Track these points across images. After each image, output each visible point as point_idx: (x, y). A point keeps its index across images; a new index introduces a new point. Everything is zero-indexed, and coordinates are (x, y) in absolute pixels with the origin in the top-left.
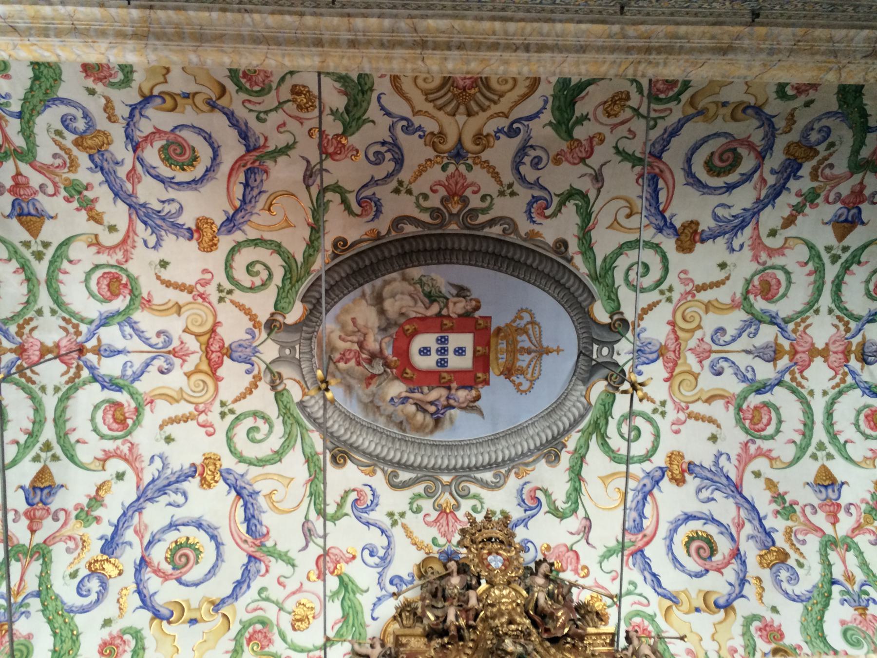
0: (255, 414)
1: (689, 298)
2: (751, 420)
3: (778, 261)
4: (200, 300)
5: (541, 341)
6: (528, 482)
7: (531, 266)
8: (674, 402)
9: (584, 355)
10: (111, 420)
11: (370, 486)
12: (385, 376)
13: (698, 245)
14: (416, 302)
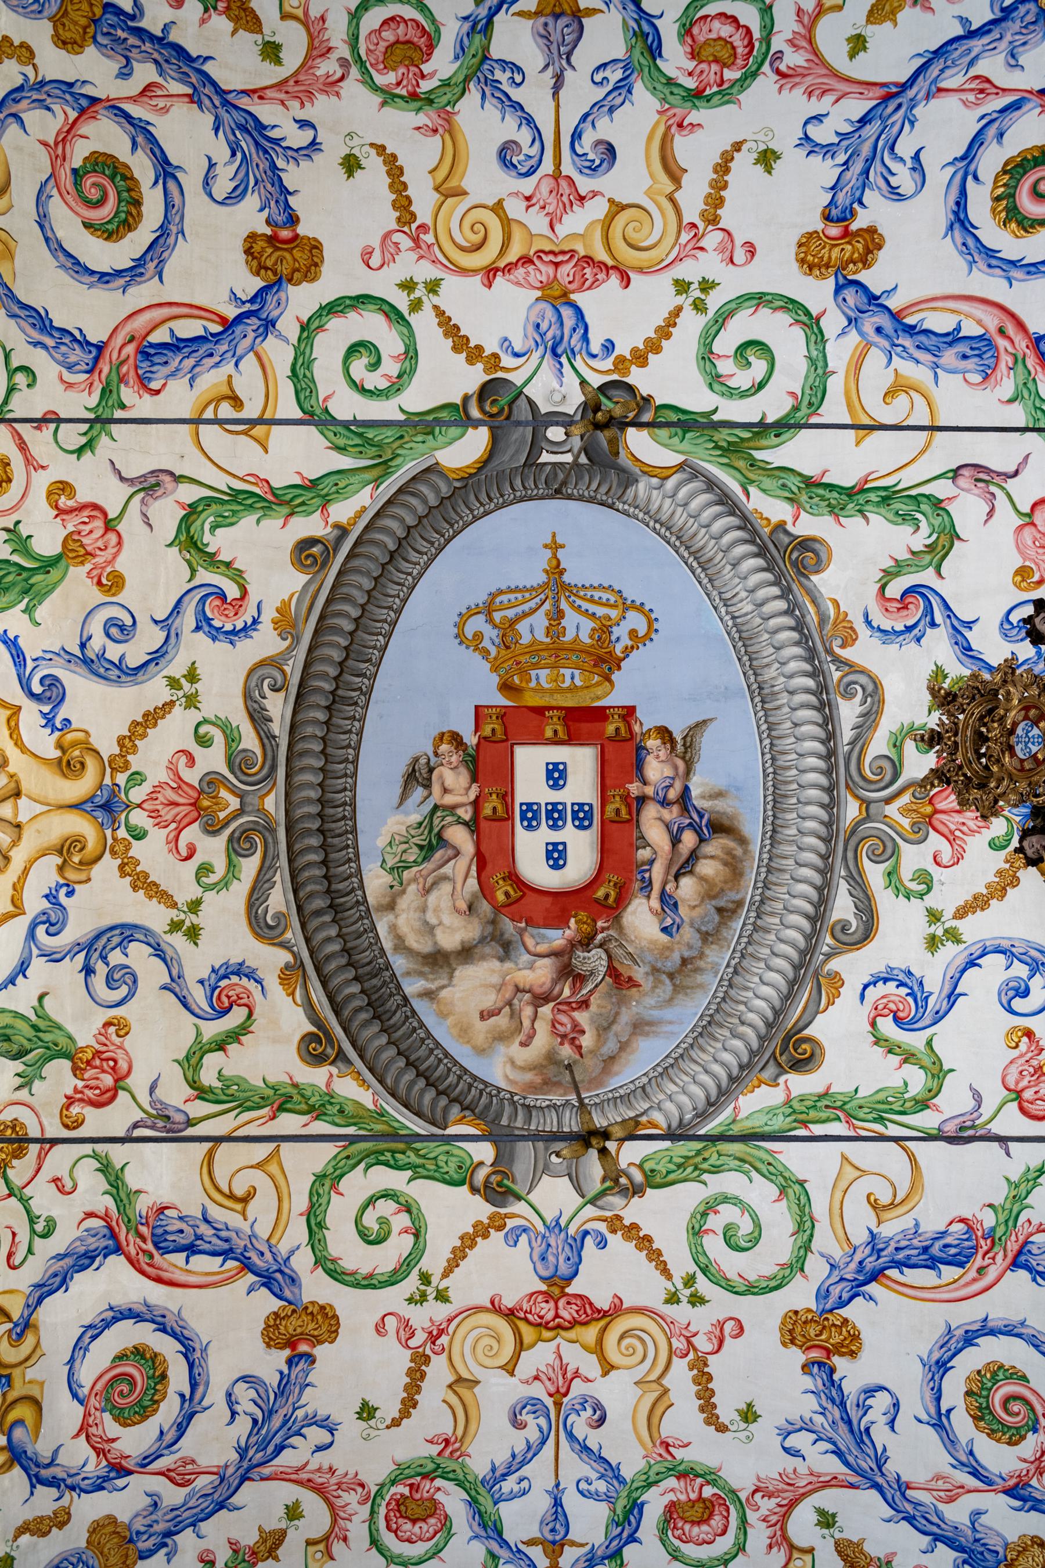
0: (697, 1232)
1: (429, 238)
2: (724, 65)
3: (337, 32)
4: (444, 1340)
5: (533, 588)
7: (356, 620)
8: (679, 259)
9: (564, 483)
10: (705, 1528)
13: (301, 230)
14: (445, 878)
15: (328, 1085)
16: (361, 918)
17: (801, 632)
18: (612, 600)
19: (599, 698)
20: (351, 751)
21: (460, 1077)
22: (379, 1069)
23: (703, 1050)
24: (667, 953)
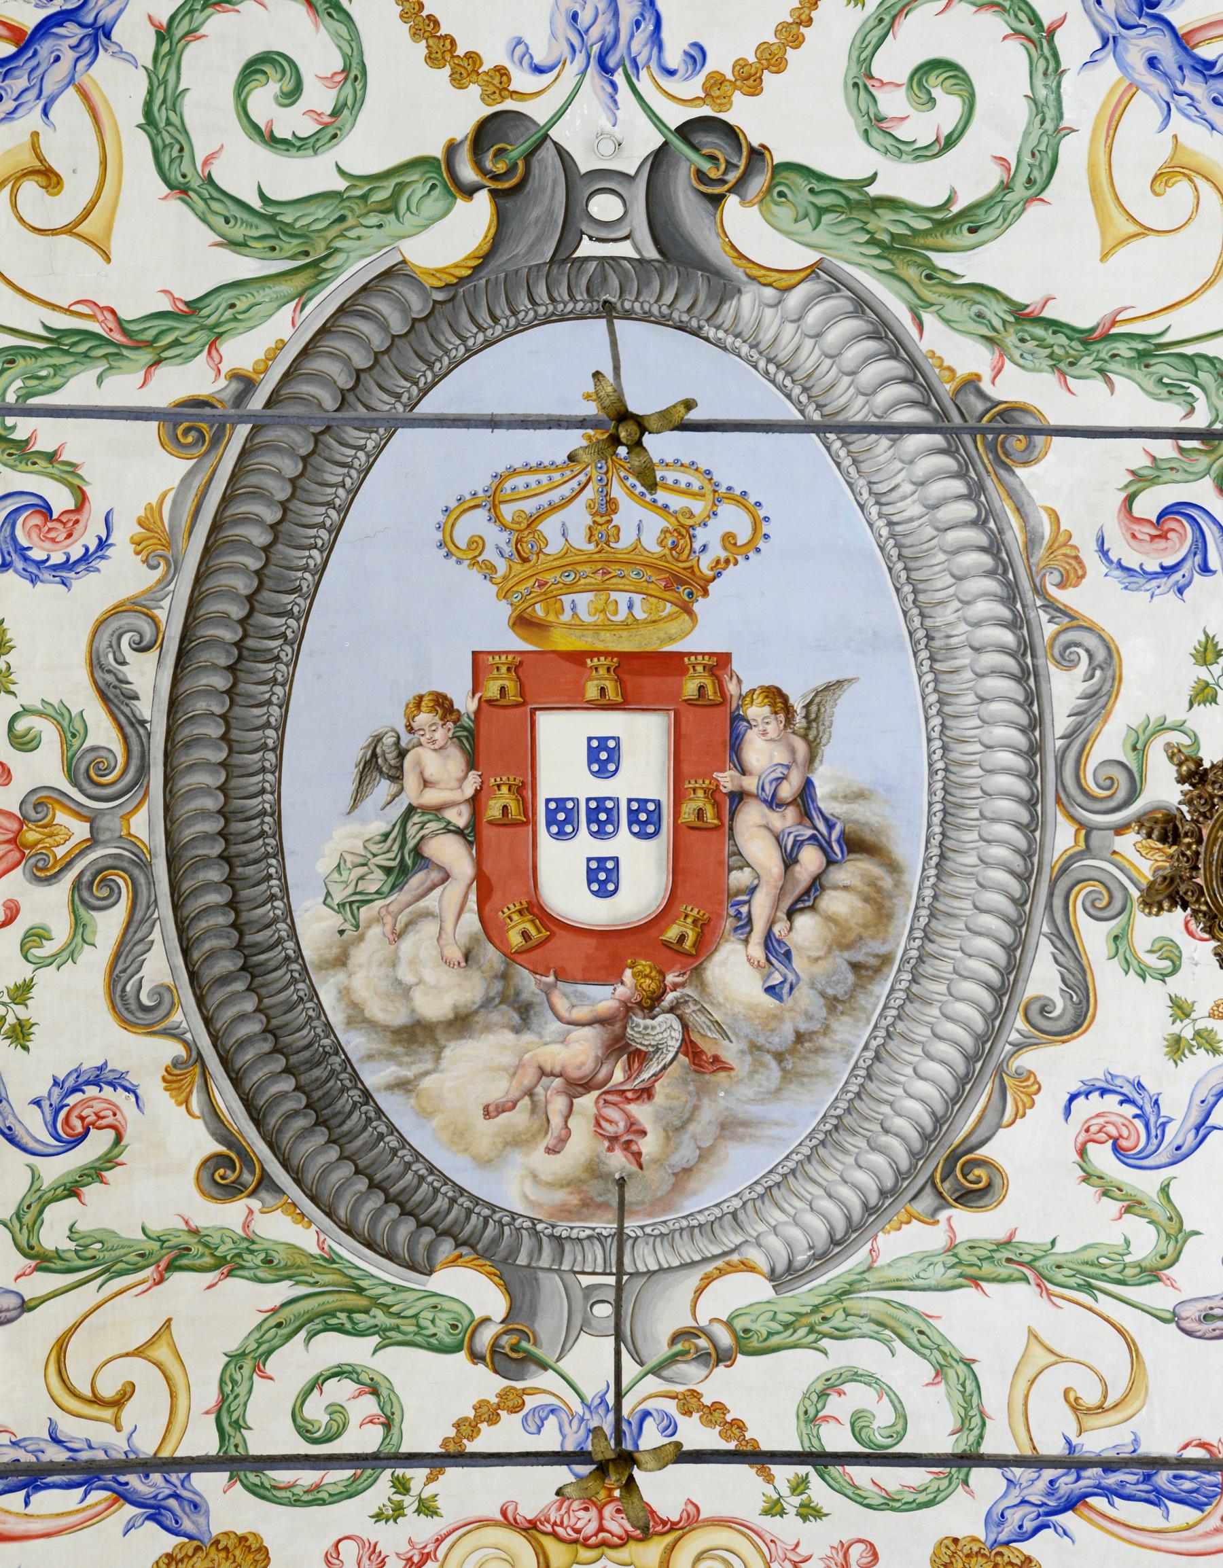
6: (1101, 542)
11: (1073, 1097)
12: (689, 1010)
14: (427, 914)
15: (246, 1225)
16: (294, 981)
17: (996, 556)
18: (696, 485)
19: (672, 639)
20: (270, 733)
21: (453, 1201)
22: (327, 1192)
23: (823, 1162)
24: (774, 1024)
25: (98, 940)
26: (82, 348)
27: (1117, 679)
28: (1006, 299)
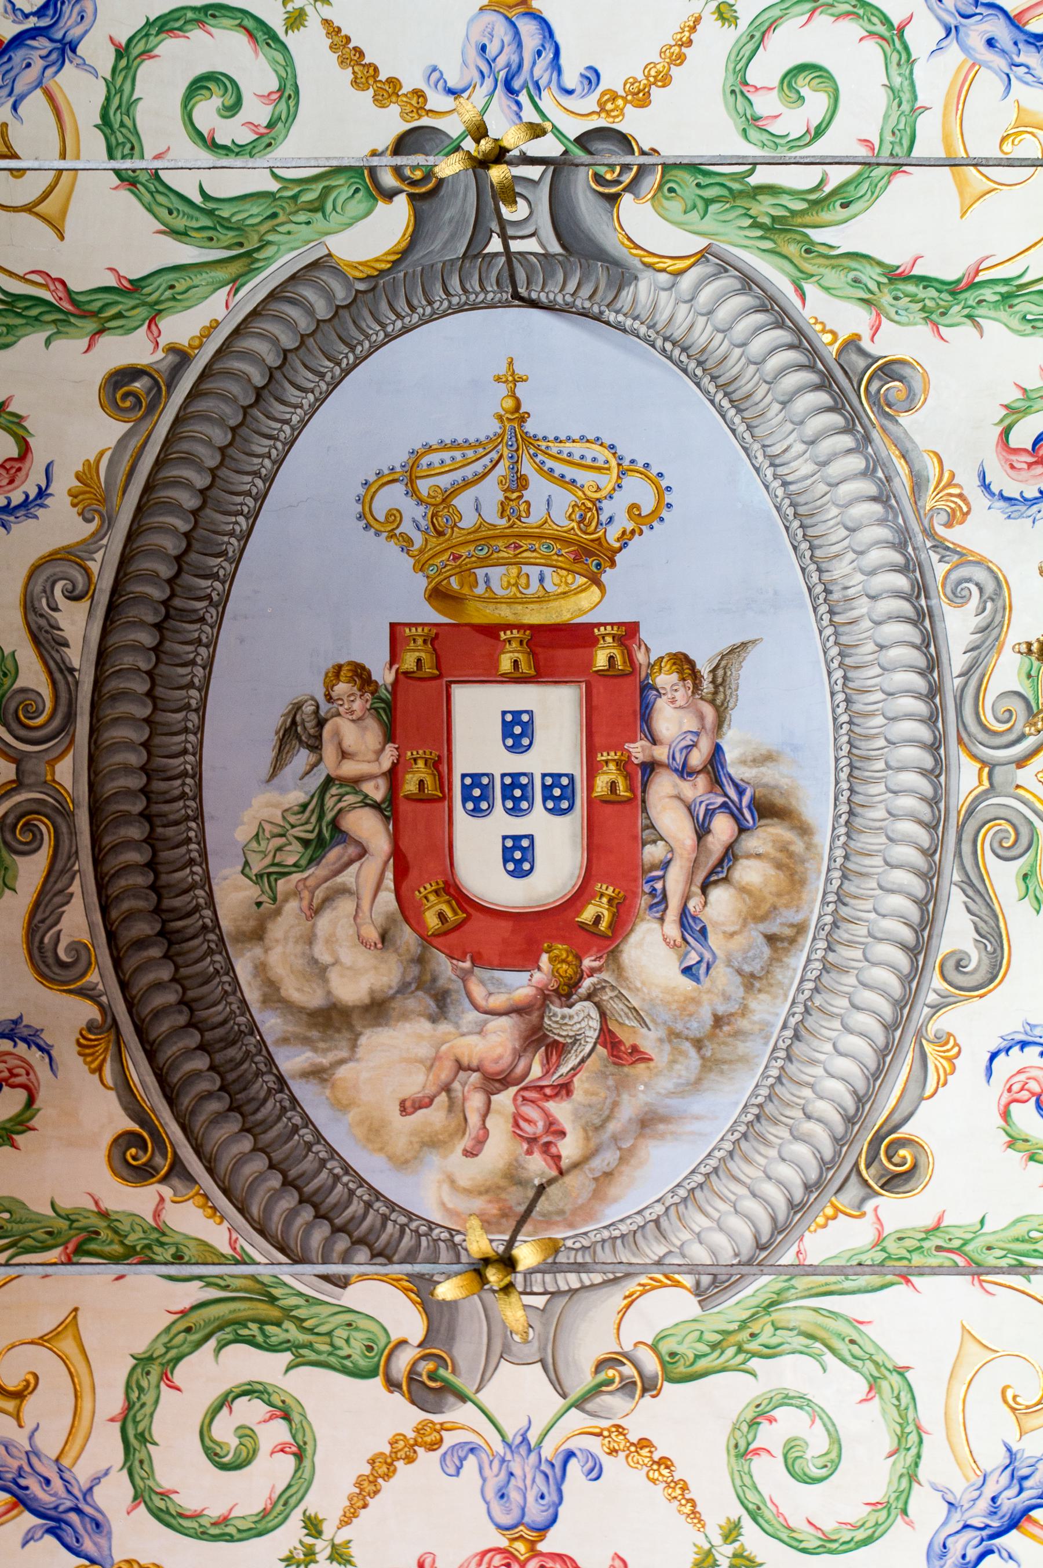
5: (479, 443)
6: (983, 476)
11: (993, 1056)
12: (606, 996)
14: (344, 891)
15: (157, 1214)
16: (211, 952)
20: (193, 693)
21: (369, 1205)
24: (692, 1008)
25: (19, 885)
26: (34, 312)
27: (1006, 609)
28: (879, 264)
